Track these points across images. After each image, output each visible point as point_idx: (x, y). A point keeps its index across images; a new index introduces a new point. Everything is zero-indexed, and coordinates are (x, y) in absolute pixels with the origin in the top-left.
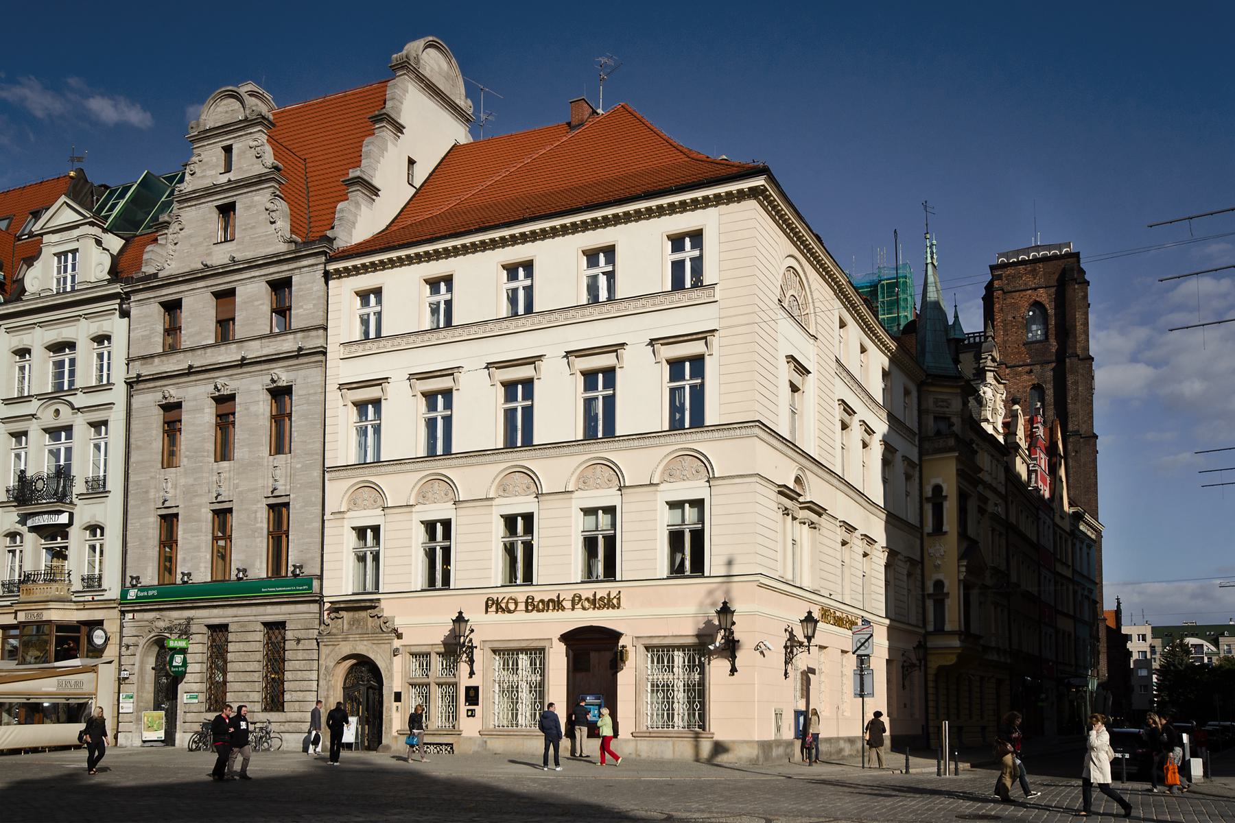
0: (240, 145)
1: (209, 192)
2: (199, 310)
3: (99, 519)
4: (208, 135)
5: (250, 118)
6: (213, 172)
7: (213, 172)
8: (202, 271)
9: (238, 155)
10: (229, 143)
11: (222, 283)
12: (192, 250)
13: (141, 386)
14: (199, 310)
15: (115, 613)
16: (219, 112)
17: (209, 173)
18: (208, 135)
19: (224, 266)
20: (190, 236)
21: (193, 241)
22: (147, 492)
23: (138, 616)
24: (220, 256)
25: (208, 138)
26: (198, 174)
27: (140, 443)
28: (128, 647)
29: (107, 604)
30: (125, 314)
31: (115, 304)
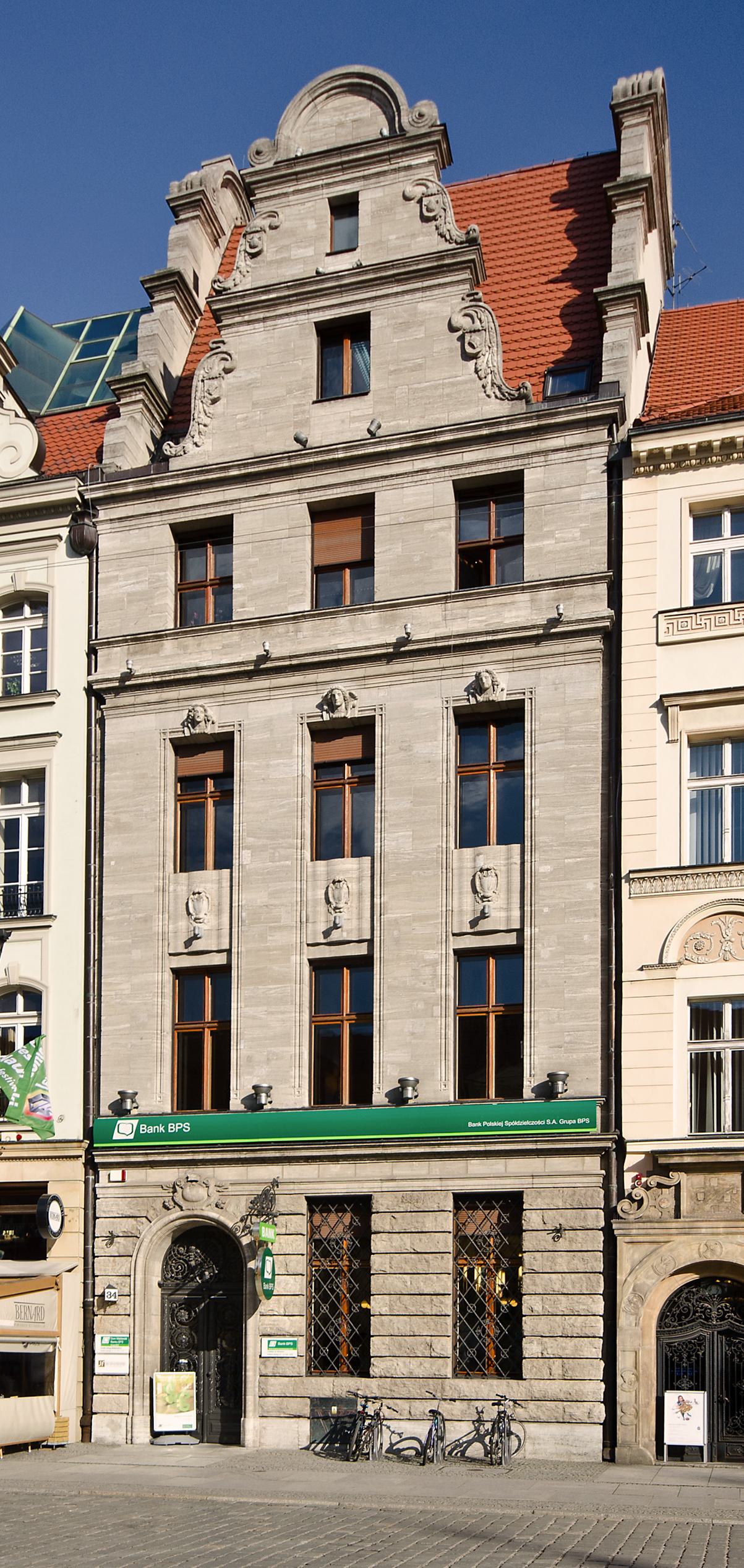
0: (378, 193)
1: (302, 290)
2: (272, 552)
4: (295, 170)
5: (412, 131)
6: (310, 252)
7: (310, 252)
8: (289, 455)
9: (374, 215)
10: (348, 188)
12: (258, 415)
13: (126, 699)
14: (272, 552)
15: (77, 1168)
16: (322, 120)
17: (297, 253)
18: (295, 170)
19: (350, 445)
20: (250, 386)
21: (258, 395)
22: (147, 920)
23: (133, 1175)
24: (338, 423)
25: (296, 177)
26: (269, 254)
28: (111, 1238)
29: (53, 1149)
30: (83, 546)
31: (61, 526)
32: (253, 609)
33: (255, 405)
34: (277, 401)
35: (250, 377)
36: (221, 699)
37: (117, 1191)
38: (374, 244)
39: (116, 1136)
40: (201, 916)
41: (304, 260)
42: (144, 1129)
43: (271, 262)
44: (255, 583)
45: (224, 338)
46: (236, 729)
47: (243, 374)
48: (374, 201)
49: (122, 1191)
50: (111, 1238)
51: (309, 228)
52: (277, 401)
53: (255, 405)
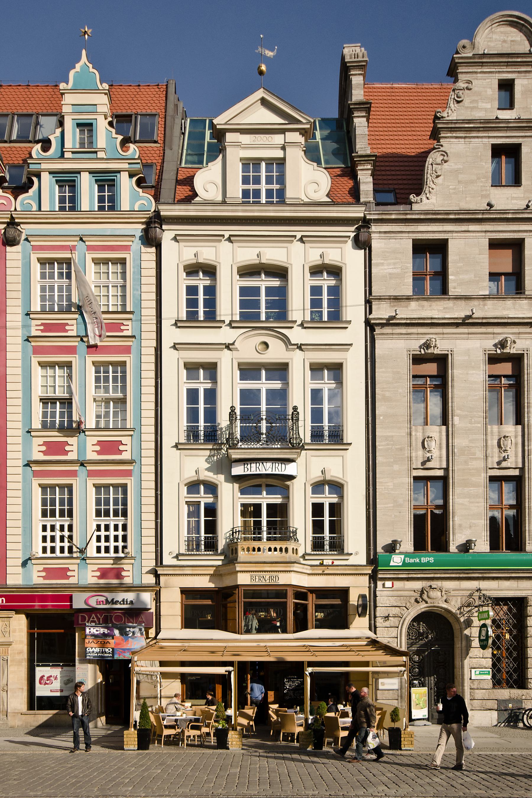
0: (525, 82)
1: (487, 126)
3: (335, 473)
4: (483, 60)
8: (483, 212)
9: (524, 93)
10: (510, 76)
11: (507, 231)
12: (461, 188)
17: (481, 105)
18: (483, 60)
19: (517, 212)
20: (457, 172)
21: (461, 177)
23: (398, 584)
25: (482, 64)
26: (467, 102)
27: (387, 394)
28: (387, 617)
32: (460, 290)
33: (459, 182)
34: (472, 182)
35: (456, 167)
36: (442, 336)
37: (388, 593)
38: (523, 108)
39: (392, 564)
40: (432, 449)
41: (486, 110)
42: (408, 560)
43: (468, 107)
44: (461, 277)
45: (442, 143)
46: (449, 353)
47: (453, 164)
48: (523, 86)
49: (391, 593)
50: (387, 617)
51: (488, 93)
52: (472, 182)
53: (459, 182)
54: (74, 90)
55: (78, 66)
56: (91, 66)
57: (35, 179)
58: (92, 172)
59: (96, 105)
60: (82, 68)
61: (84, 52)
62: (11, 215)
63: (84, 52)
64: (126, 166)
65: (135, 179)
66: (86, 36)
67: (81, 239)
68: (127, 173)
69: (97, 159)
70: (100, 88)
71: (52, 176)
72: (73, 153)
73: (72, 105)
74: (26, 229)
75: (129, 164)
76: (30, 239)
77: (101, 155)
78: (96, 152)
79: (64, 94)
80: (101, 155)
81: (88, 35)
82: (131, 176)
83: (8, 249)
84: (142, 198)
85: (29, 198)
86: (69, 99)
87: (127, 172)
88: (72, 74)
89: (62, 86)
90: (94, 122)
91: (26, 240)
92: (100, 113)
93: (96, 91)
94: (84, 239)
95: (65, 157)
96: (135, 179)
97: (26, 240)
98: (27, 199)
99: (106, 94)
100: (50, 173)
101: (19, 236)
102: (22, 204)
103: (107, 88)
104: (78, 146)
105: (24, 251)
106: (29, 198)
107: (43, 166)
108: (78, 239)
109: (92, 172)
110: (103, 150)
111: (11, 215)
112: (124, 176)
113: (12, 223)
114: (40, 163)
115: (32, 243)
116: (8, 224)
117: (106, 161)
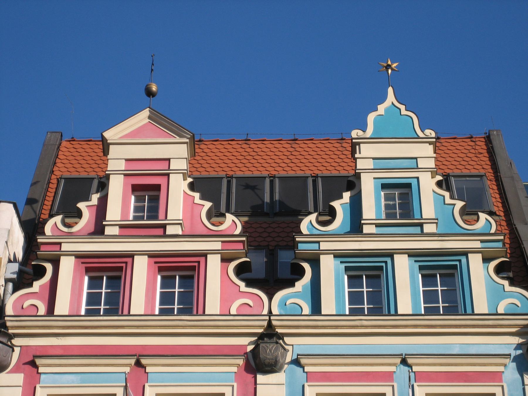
54: (375, 139)
55: (382, 109)
56: (402, 107)
57: (307, 266)
58: (412, 254)
59: (416, 158)
60: (386, 110)
61: (390, 90)
62: (270, 321)
63: (390, 90)
64: (478, 245)
65: (493, 264)
66: (390, 71)
67: (404, 362)
68: (479, 256)
69: (422, 234)
70: (421, 134)
71: (339, 260)
72: (378, 226)
73: (374, 159)
74: (295, 345)
75: (482, 241)
76: (303, 361)
77: (429, 228)
78: (421, 225)
79: (359, 144)
80: (429, 228)
81: (392, 69)
82: (486, 260)
83: (261, 378)
84: (511, 295)
85: (296, 295)
86: (366, 151)
87: (480, 255)
88: (371, 118)
89: (355, 133)
90: (414, 182)
91: (296, 362)
92: (425, 170)
93: (415, 139)
94: (410, 361)
95: (365, 231)
96: (493, 264)
97: (296, 362)
98: (294, 296)
99: (430, 143)
100: (336, 256)
101: (284, 356)
102: (283, 304)
103: (433, 135)
104: (383, 216)
105: (290, 384)
106: (296, 295)
107: (324, 246)
108: (398, 361)
109: (412, 254)
110: (435, 221)
111: (270, 321)
112: (475, 260)
113: (270, 334)
114: (318, 242)
115: (307, 369)
116: (261, 337)
117: (440, 238)
